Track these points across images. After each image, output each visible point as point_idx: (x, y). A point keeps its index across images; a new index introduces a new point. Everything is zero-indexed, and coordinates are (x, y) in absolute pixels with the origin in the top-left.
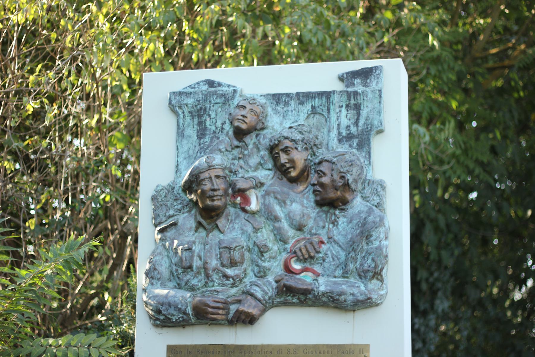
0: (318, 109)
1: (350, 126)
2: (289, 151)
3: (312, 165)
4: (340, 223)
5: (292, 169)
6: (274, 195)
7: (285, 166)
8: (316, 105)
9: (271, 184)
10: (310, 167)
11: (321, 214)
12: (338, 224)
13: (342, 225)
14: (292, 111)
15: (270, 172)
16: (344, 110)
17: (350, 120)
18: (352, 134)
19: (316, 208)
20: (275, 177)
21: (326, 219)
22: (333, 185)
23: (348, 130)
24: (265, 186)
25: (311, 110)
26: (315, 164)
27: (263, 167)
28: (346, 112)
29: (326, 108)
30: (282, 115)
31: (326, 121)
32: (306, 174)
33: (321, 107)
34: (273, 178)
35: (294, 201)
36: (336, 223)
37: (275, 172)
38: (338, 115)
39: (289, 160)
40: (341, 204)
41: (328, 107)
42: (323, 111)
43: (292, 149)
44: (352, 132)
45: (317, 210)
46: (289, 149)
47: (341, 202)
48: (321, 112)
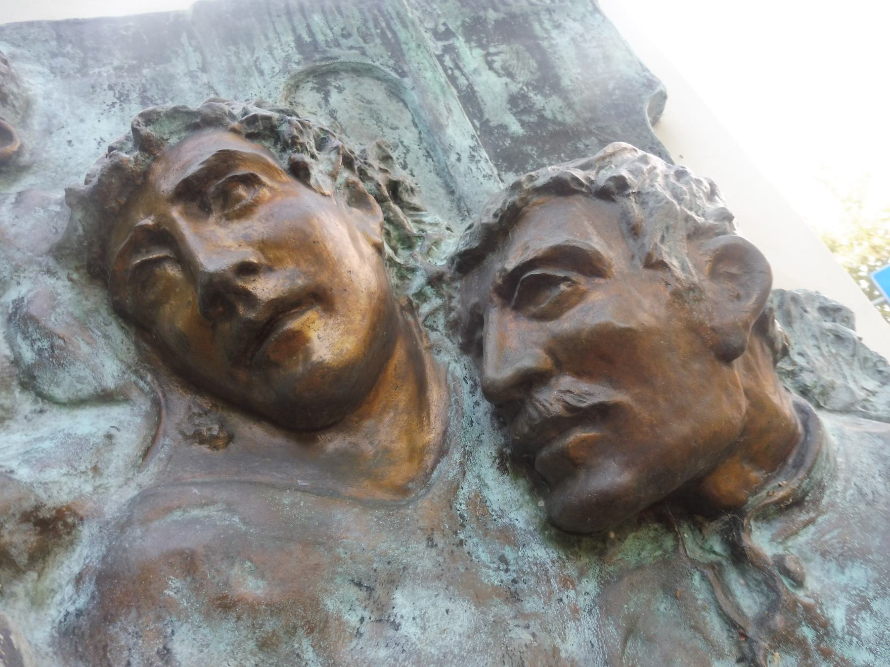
0: (335, 51)
1: (525, 97)
2: (250, 181)
3: (421, 295)
4: (838, 616)
5: (311, 315)
6: (197, 587)
7: (249, 298)
8: (320, 38)
9: (145, 497)
10: (412, 308)
11: (632, 604)
12: (823, 627)
13: (867, 627)
14: (192, 75)
15: (117, 413)
16: (460, 42)
17: (510, 75)
18: (554, 121)
19: (571, 570)
20: (166, 444)
21: (698, 629)
22: (695, 329)
23: (528, 111)
24: (86, 532)
25: (297, 57)
26: (436, 280)
27: (41, 396)
28: (478, 52)
29: (378, 41)
30: (134, 95)
31: (395, 92)
32: (400, 354)
33: (351, 42)
34: (146, 453)
35: (393, 582)
36: (807, 633)
37: (158, 410)
38: (448, 61)
39: (263, 246)
40: (755, 475)
41: (383, 35)
42: (364, 53)
43: (268, 169)
44: (548, 114)
45: (590, 585)
46: (242, 171)
47: (755, 461)
48: (353, 57)
